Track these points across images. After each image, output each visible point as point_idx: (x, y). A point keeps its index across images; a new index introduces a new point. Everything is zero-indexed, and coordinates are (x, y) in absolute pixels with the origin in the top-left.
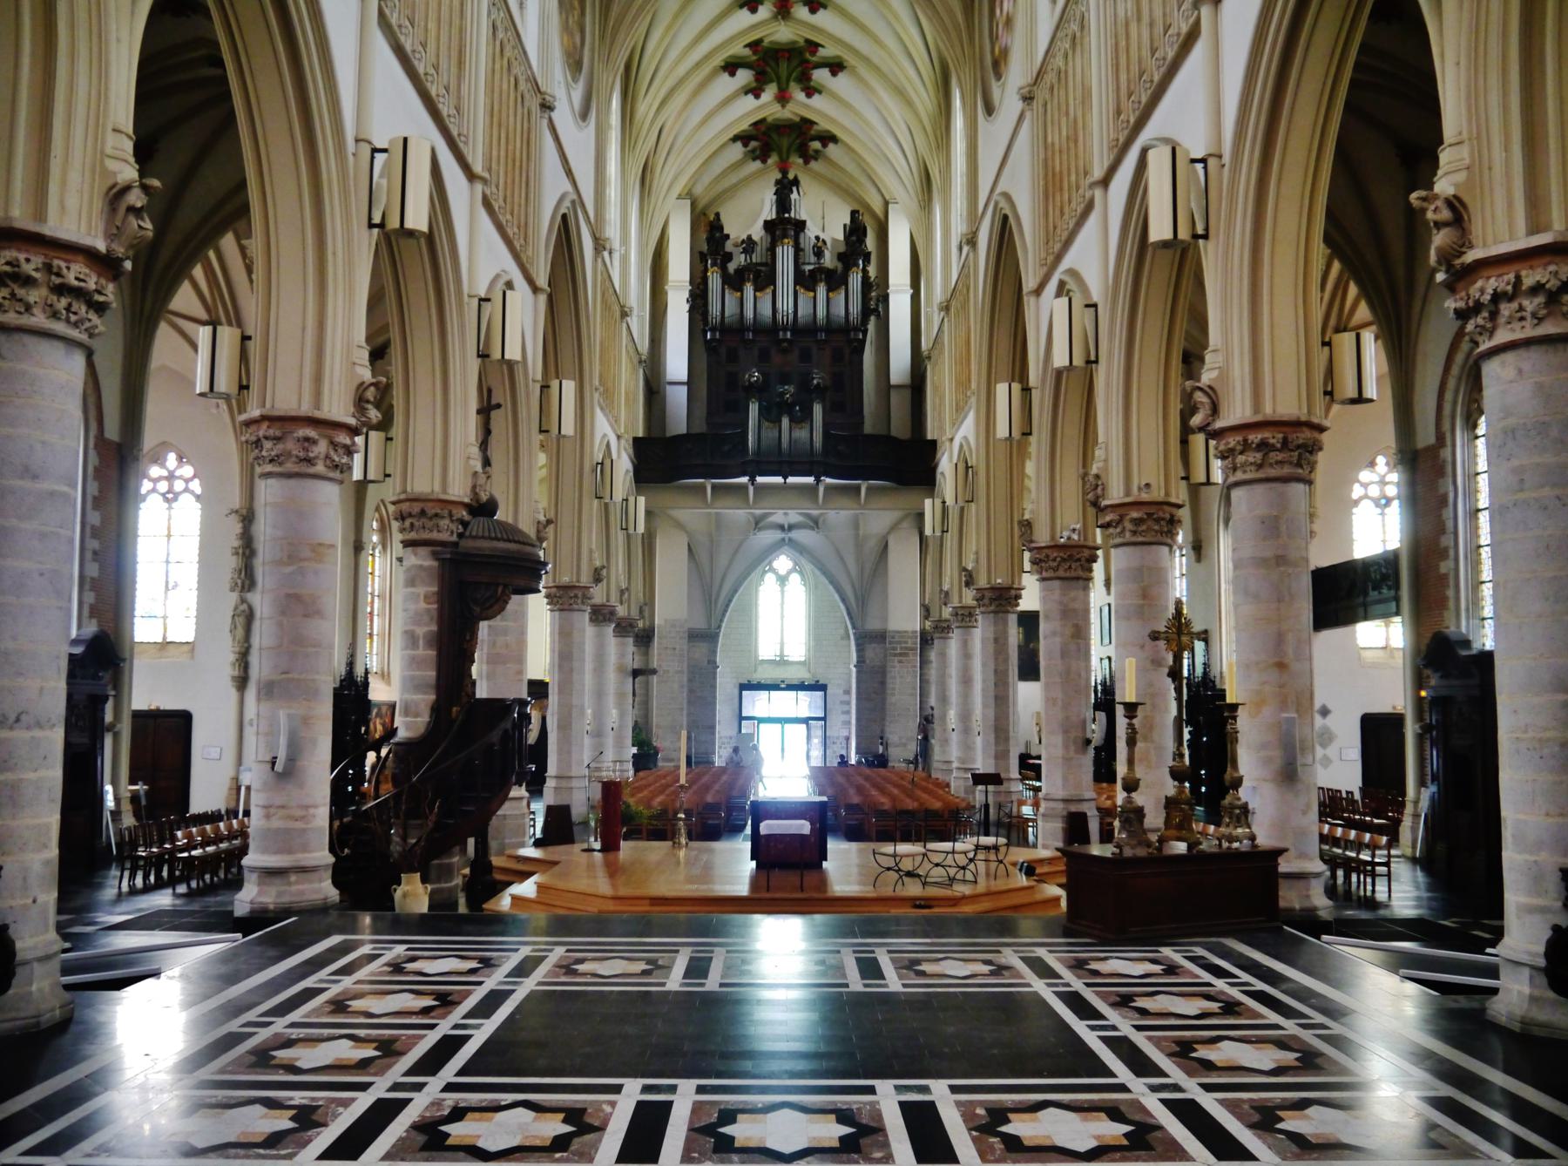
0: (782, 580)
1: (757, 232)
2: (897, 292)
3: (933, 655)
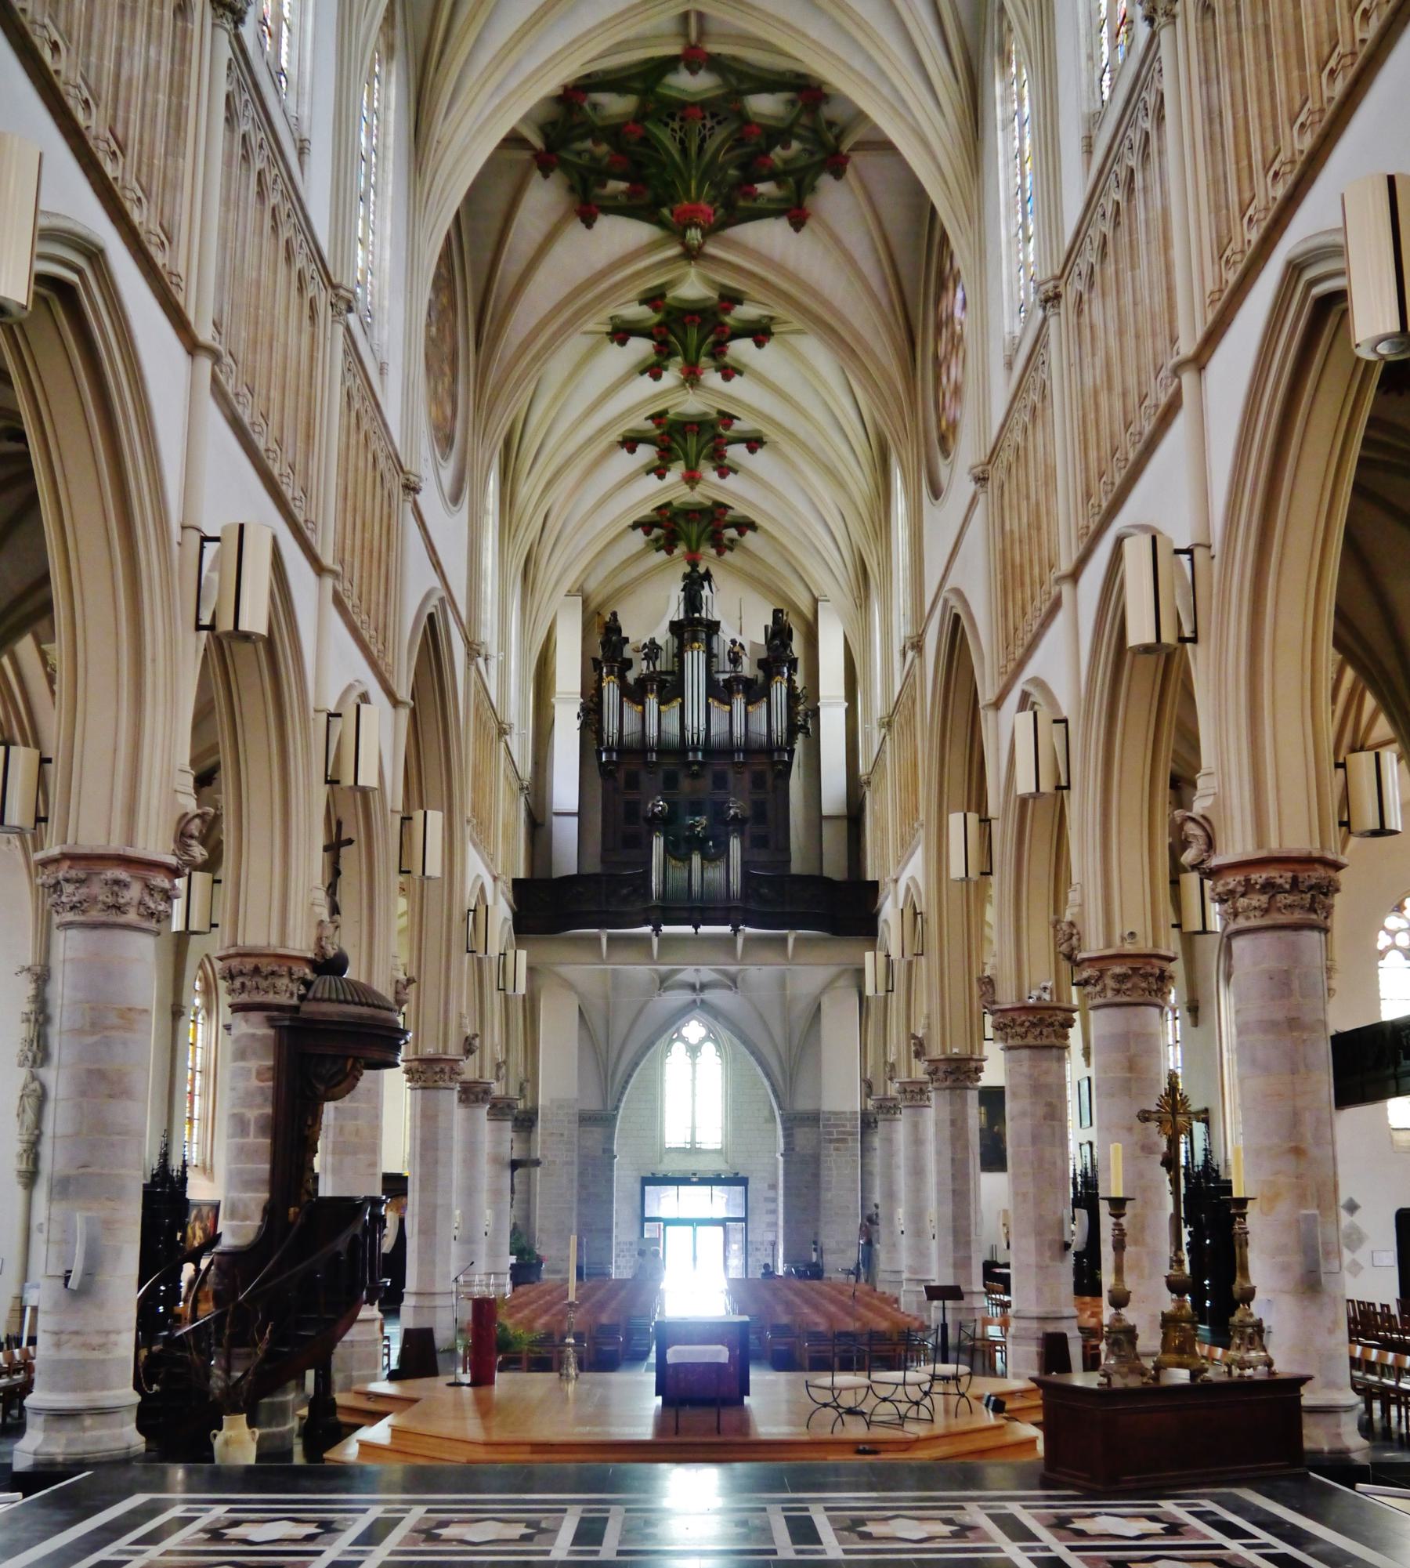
0: (694, 1050)
1: (662, 636)
2: (829, 705)
3: (877, 1141)
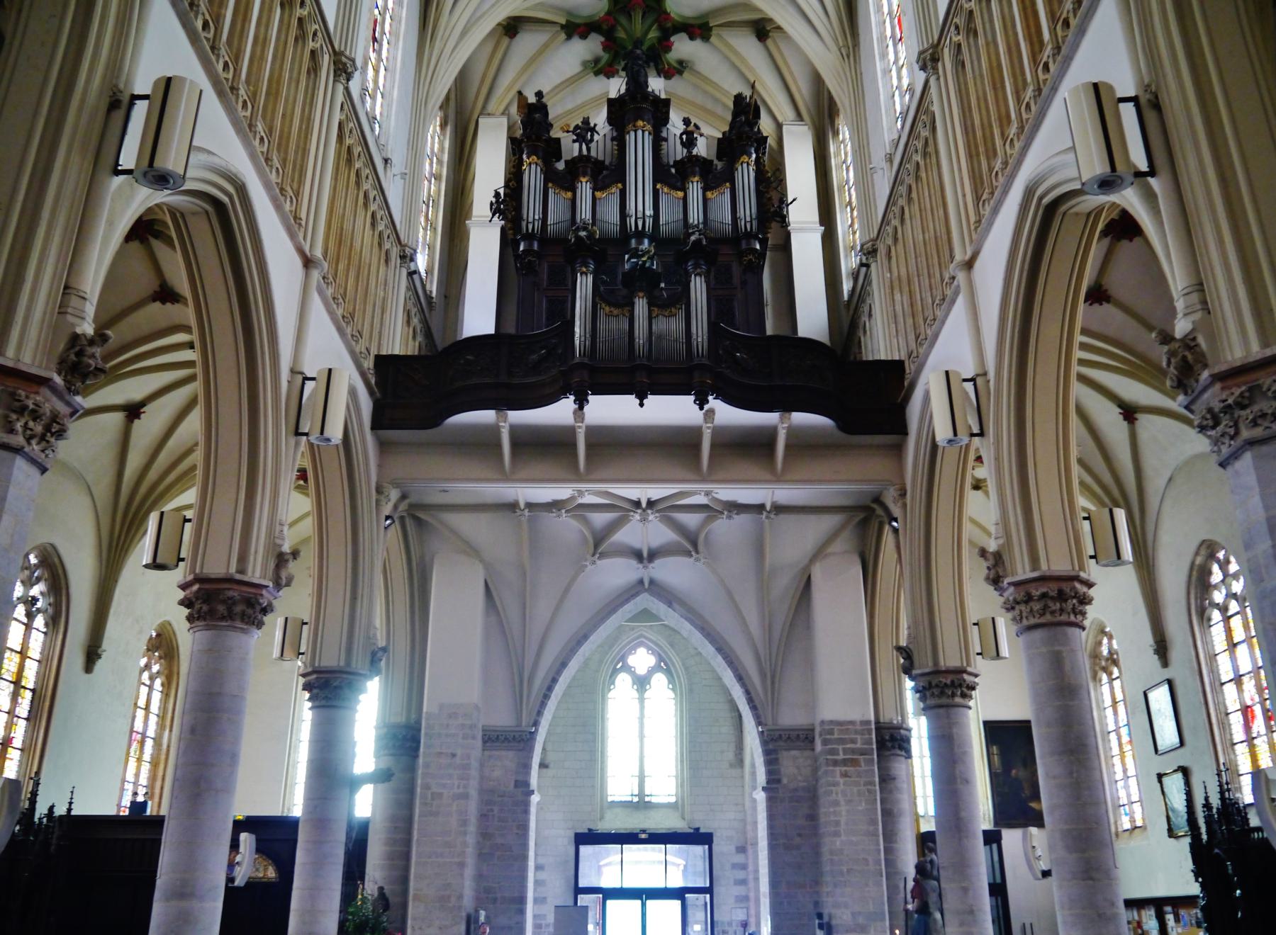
0: (642, 683)
2: (801, 230)
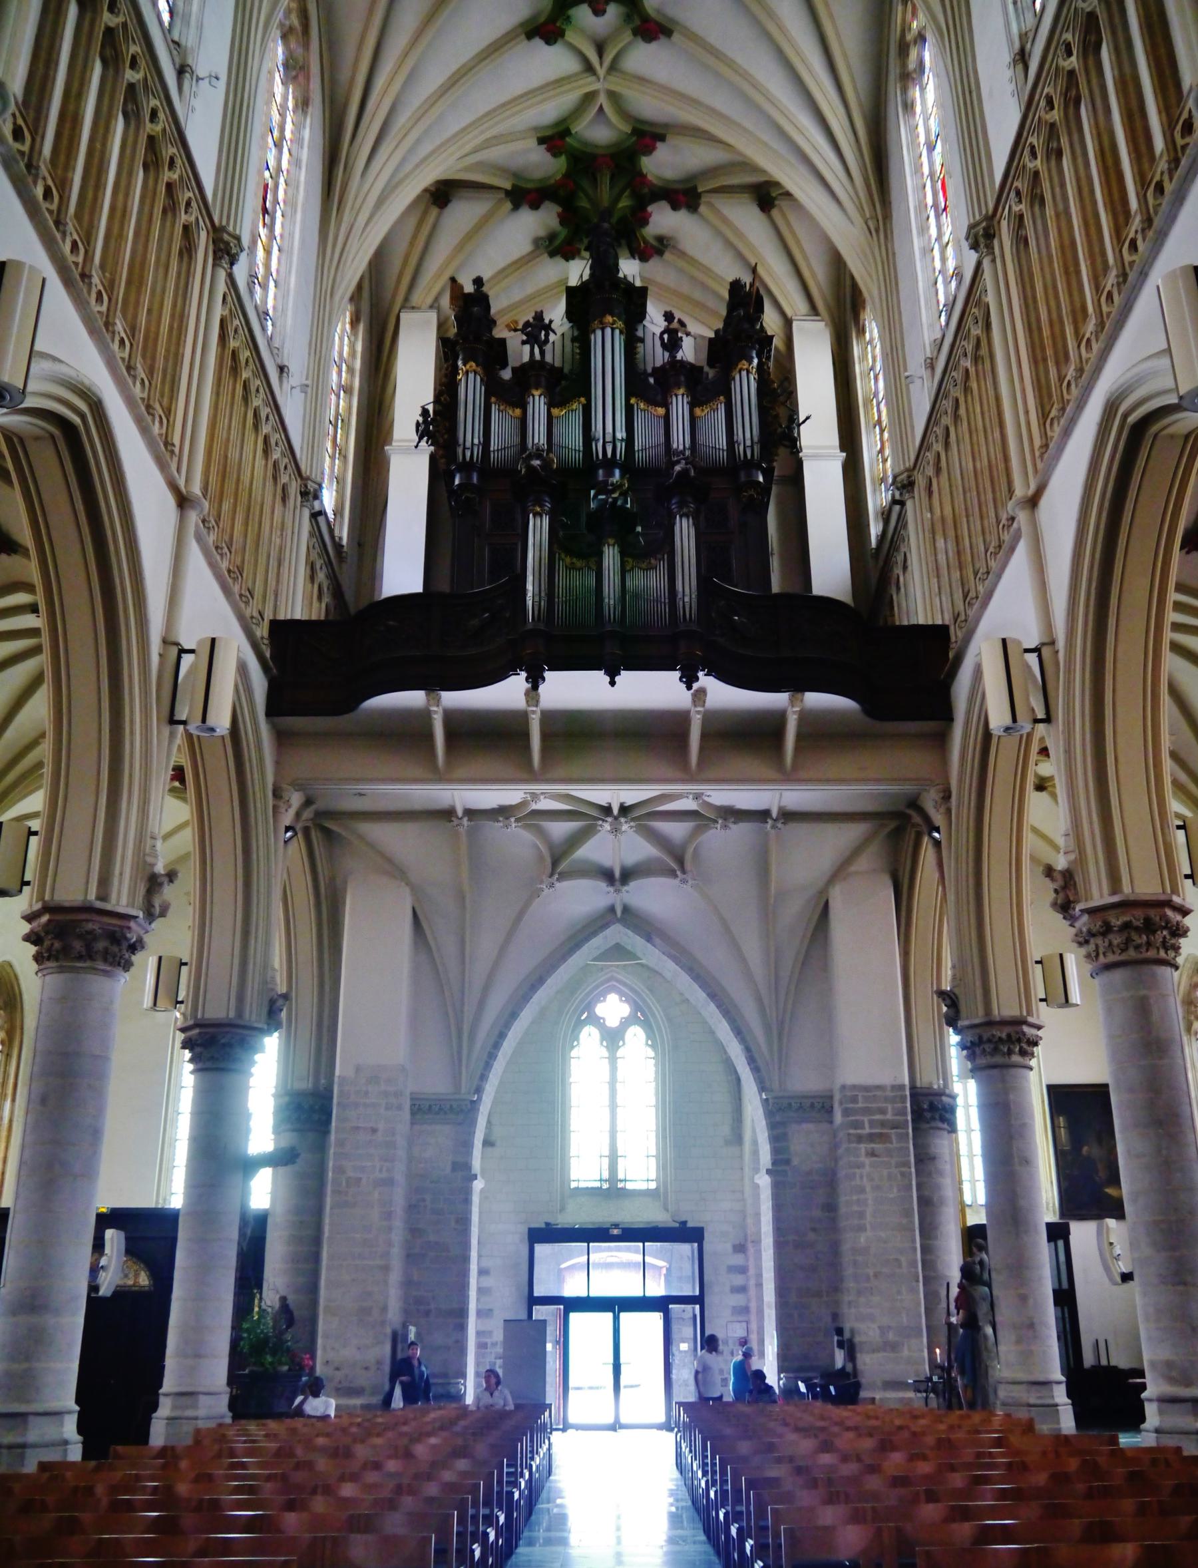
0: (613, 1038)
2: (816, 457)
